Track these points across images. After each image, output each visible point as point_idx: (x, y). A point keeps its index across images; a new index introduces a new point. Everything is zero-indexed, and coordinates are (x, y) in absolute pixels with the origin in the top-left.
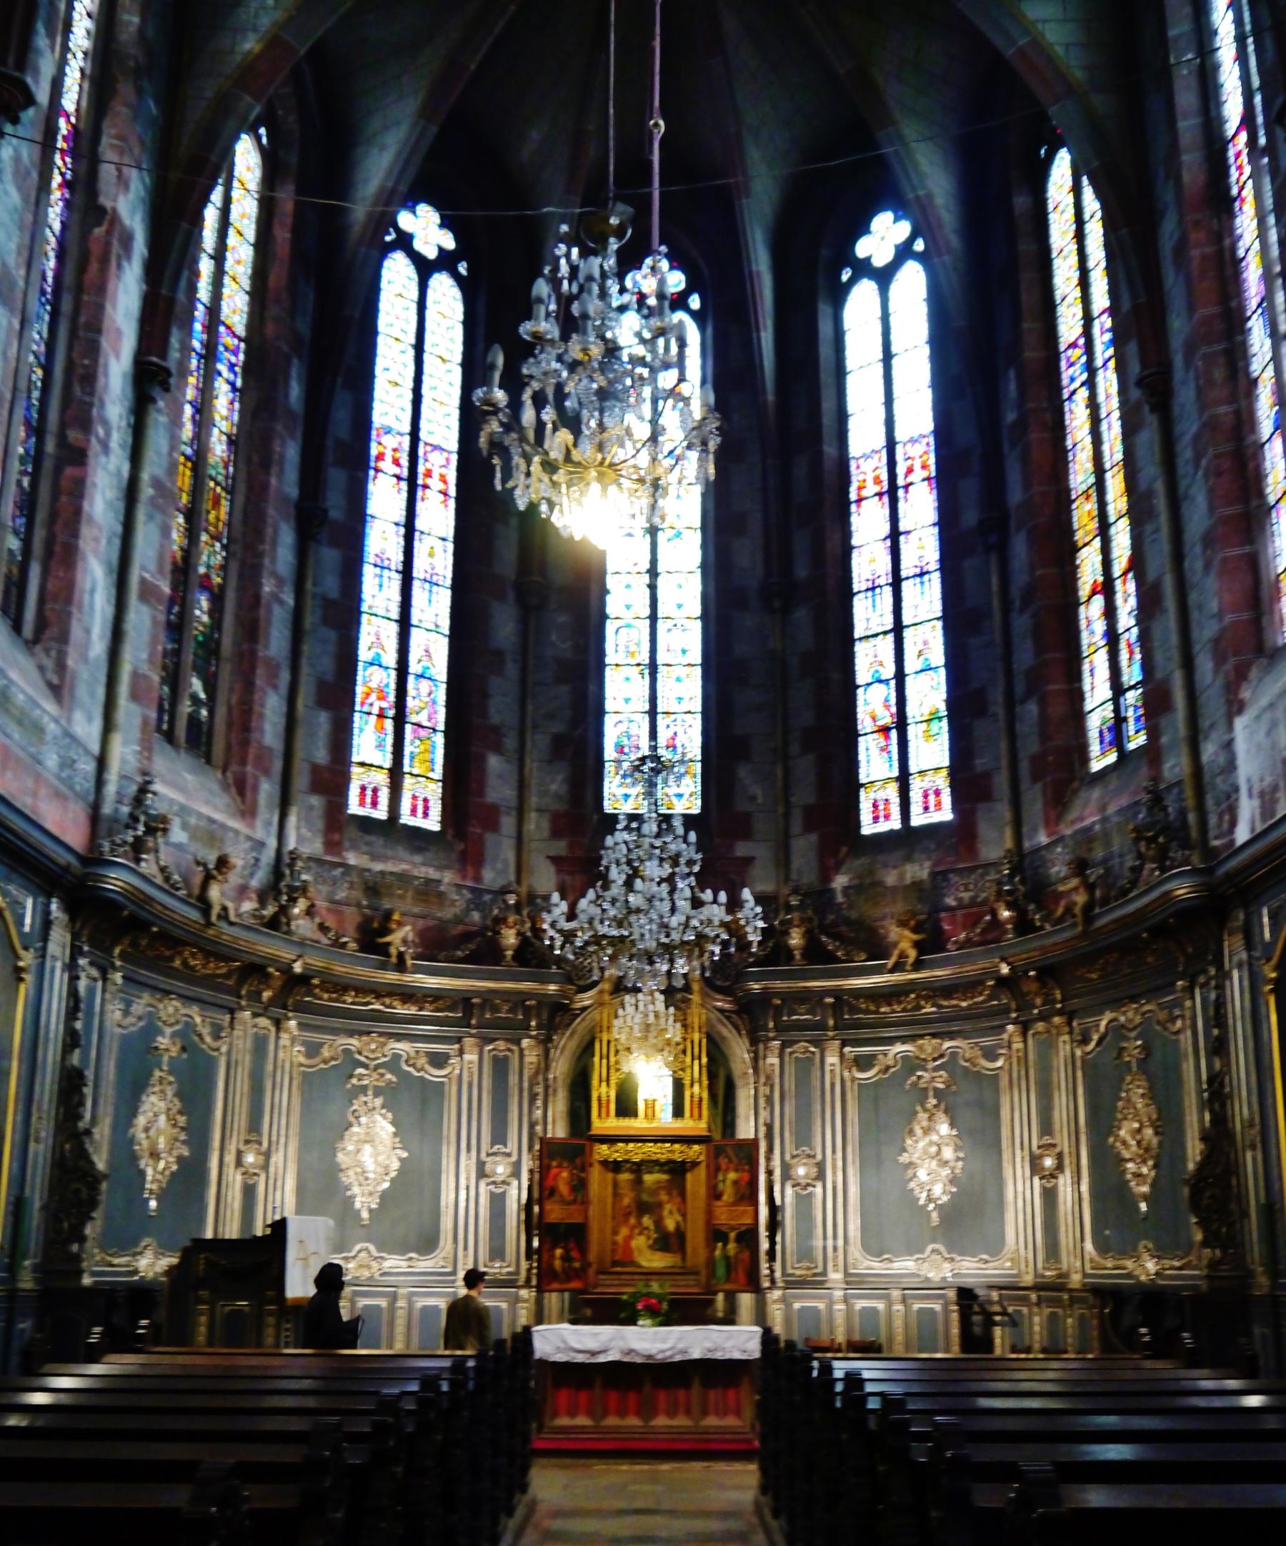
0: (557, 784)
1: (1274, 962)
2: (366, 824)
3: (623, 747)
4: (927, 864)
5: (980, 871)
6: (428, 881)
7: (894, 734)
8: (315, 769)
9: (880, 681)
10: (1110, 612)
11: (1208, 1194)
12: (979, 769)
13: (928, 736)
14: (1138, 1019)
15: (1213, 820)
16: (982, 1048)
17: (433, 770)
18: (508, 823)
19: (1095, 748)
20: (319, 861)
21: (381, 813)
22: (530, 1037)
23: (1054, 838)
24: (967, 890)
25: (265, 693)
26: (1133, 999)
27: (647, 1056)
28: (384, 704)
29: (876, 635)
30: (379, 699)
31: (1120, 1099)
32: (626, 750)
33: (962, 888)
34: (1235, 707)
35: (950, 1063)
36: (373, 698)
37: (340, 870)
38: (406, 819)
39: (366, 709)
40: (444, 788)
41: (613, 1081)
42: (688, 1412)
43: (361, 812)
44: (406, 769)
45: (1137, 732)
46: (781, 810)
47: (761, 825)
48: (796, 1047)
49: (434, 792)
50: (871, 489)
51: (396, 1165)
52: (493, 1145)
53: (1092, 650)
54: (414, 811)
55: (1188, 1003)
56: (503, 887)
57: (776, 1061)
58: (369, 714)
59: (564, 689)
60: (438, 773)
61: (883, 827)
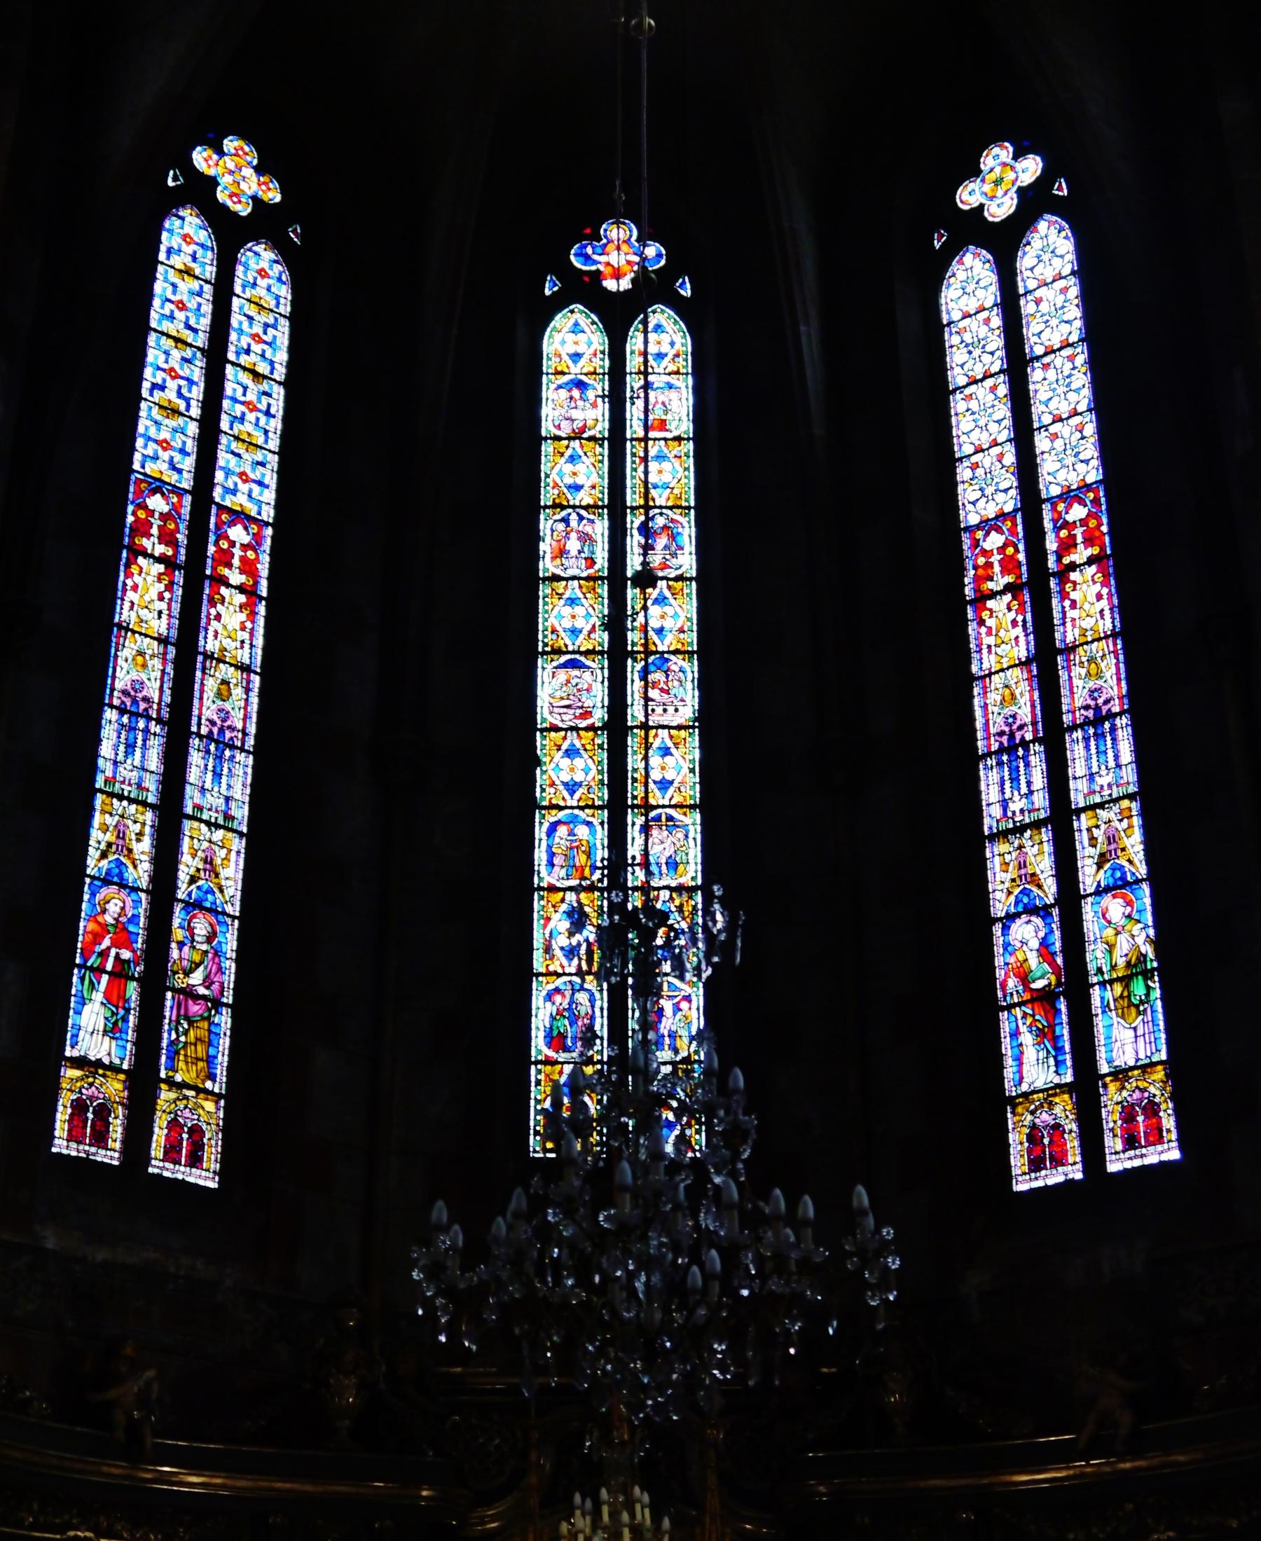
3: (562, 1036)
7: (1062, 1006)
9: (1032, 910)
13: (1128, 1006)
17: (212, 1077)
21: (110, 1156)
28: (126, 955)
29: (1020, 830)
32: (569, 1043)
36: (106, 942)
38: (158, 1166)
44: (163, 1075)
49: (210, 1113)
50: (1001, 581)
54: (171, 1154)
58: (100, 970)
61: (1053, 1177)
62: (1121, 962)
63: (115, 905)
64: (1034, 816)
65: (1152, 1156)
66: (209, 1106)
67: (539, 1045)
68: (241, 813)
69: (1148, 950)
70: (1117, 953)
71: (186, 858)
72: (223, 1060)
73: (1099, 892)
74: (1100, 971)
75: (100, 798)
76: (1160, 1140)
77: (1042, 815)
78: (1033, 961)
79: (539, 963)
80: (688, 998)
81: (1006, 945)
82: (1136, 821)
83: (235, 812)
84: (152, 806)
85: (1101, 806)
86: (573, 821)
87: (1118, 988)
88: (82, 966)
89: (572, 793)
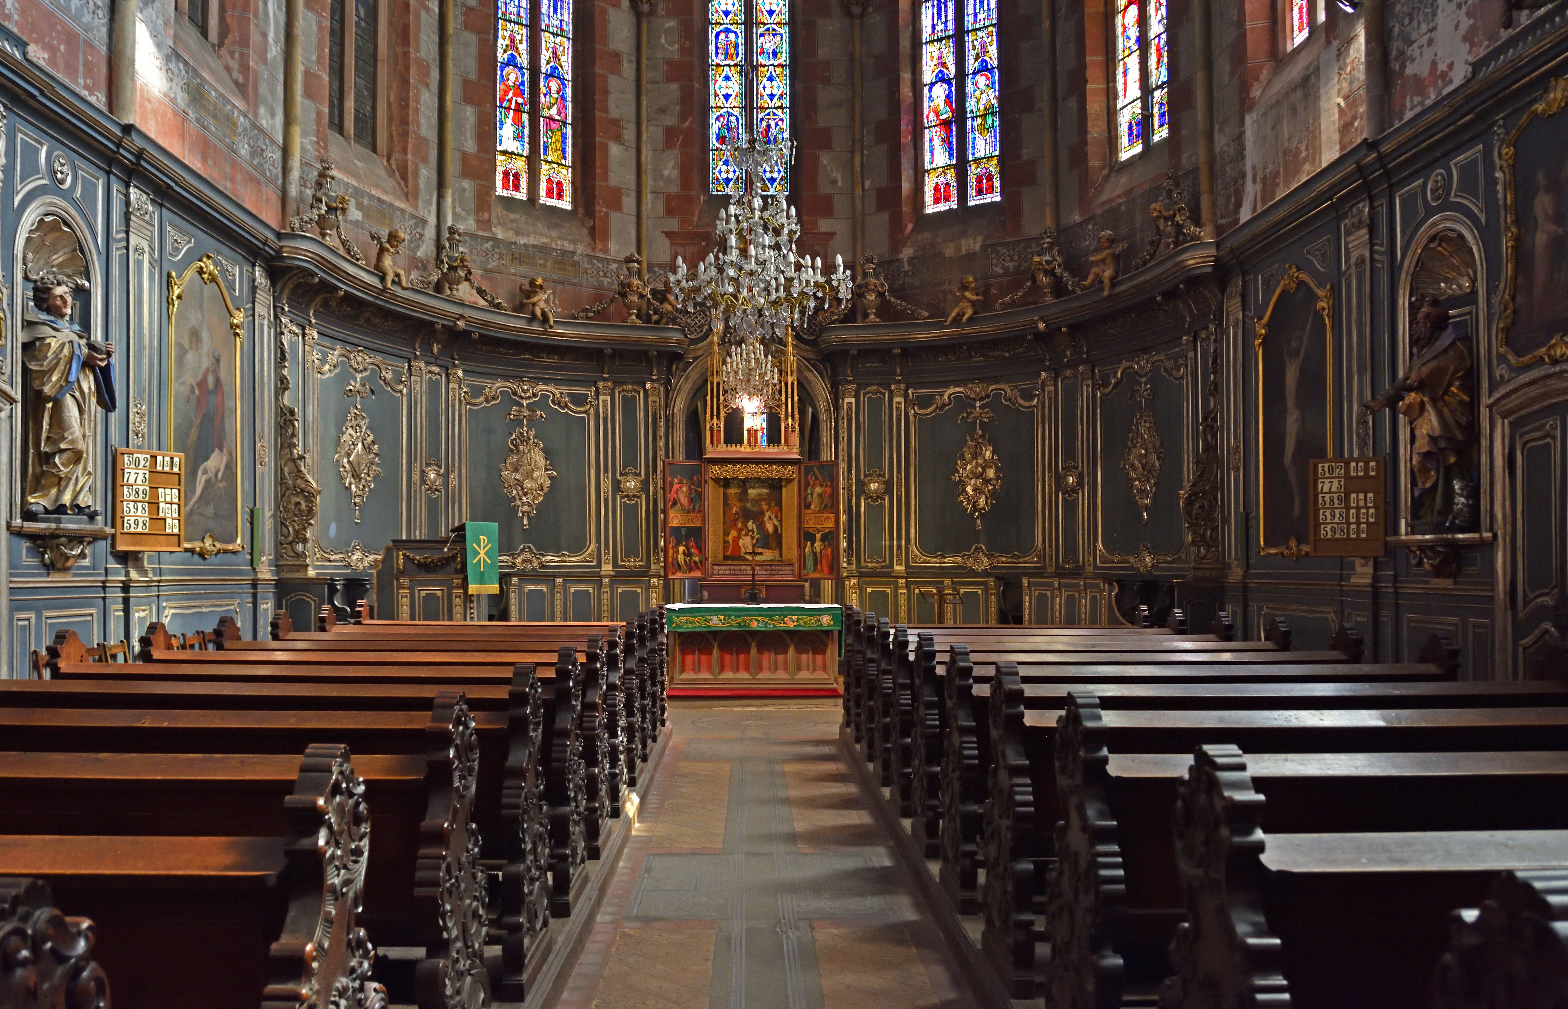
0: (670, 169)
1: (1265, 319)
2: (509, 203)
4: (980, 239)
5: (1023, 245)
6: (564, 252)
8: (465, 157)
10: (1143, 21)
11: (1197, 505)
12: (1025, 158)
13: (984, 129)
14: (1148, 367)
15: (1221, 201)
16: (1019, 390)
17: (565, 158)
18: (629, 202)
19: (1124, 140)
20: (473, 236)
21: (522, 195)
22: (652, 381)
23: (1087, 217)
24: (1012, 260)
25: (418, 90)
26: (1146, 350)
27: (750, 395)
28: (520, 100)
30: (515, 95)
31: (1131, 431)
33: (1008, 259)
34: (1245, 105)
35: (994, 402)
36: (510, 95)
37: (491, 243)
38: (544, 200)
39: (505, 104)
40: (574, 173)
41: (722, 415)
42: (786, 669)
43: (505, 193)
44: (542, 157)
45: (1161, 126)
46: (859, 191)
47: (840, 204)
48: (868, 389)
49: (565, 176)
51: (548, 482)
52: (624, 468)
53: (1127, 52)
54: (549, 194)
55: (1191, 354)
56: (626, 258)
57: (853, 400)
58: (509, 108)
59: (674, 87)
60: (568, 162)
61: (943, 207)
62: (982, 108)
63: (512, 75)
64: (947, 33)
65: (989, 199)
66: (564, 171)
67: (713, 141)
68: (569, 28)
69: (995, 102)
70: (981, 103)
71: (544, 52)
72: (569, 150)
73: (975, 73)
74: (972, 111)
75: (500, 22)
76: (992, 192)
77: (951, 33)
78: (942, 106)
79: (712, 103)
80: (782, 120)
81: (930, 97)
82: (995, 38)
83: (565, 27)
84: (526, 26)
85: (979, 29)
86: (727, 31)
87: (980, 120)
88: (501, 106)
89: (727, 16)
